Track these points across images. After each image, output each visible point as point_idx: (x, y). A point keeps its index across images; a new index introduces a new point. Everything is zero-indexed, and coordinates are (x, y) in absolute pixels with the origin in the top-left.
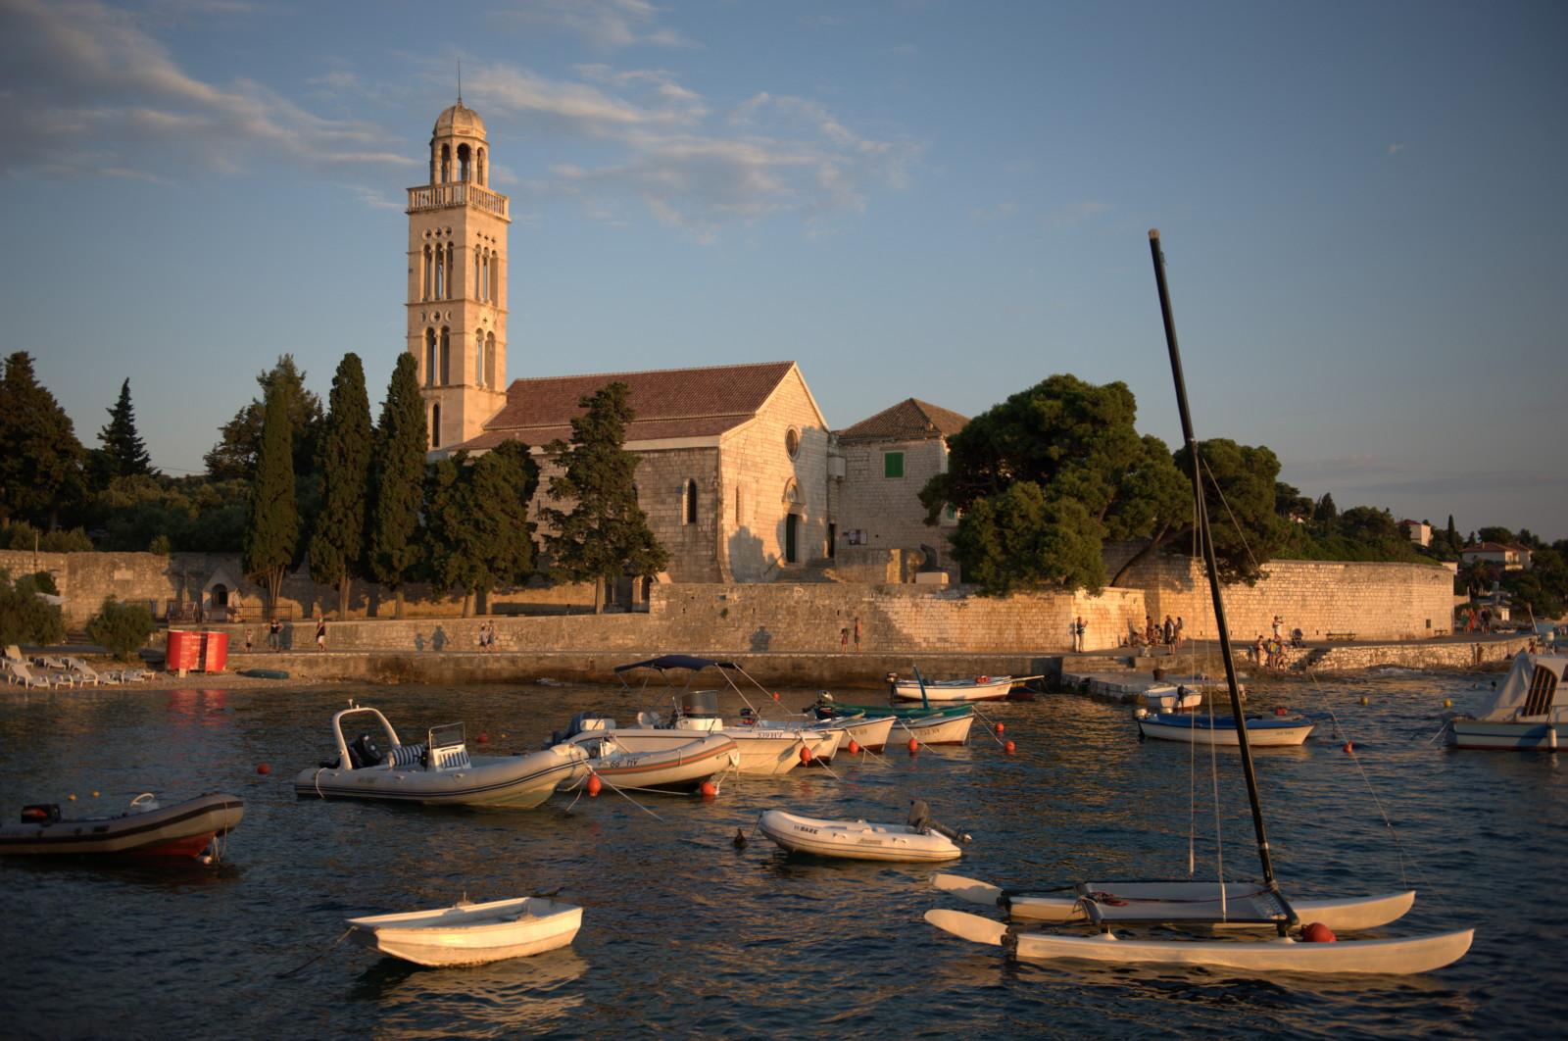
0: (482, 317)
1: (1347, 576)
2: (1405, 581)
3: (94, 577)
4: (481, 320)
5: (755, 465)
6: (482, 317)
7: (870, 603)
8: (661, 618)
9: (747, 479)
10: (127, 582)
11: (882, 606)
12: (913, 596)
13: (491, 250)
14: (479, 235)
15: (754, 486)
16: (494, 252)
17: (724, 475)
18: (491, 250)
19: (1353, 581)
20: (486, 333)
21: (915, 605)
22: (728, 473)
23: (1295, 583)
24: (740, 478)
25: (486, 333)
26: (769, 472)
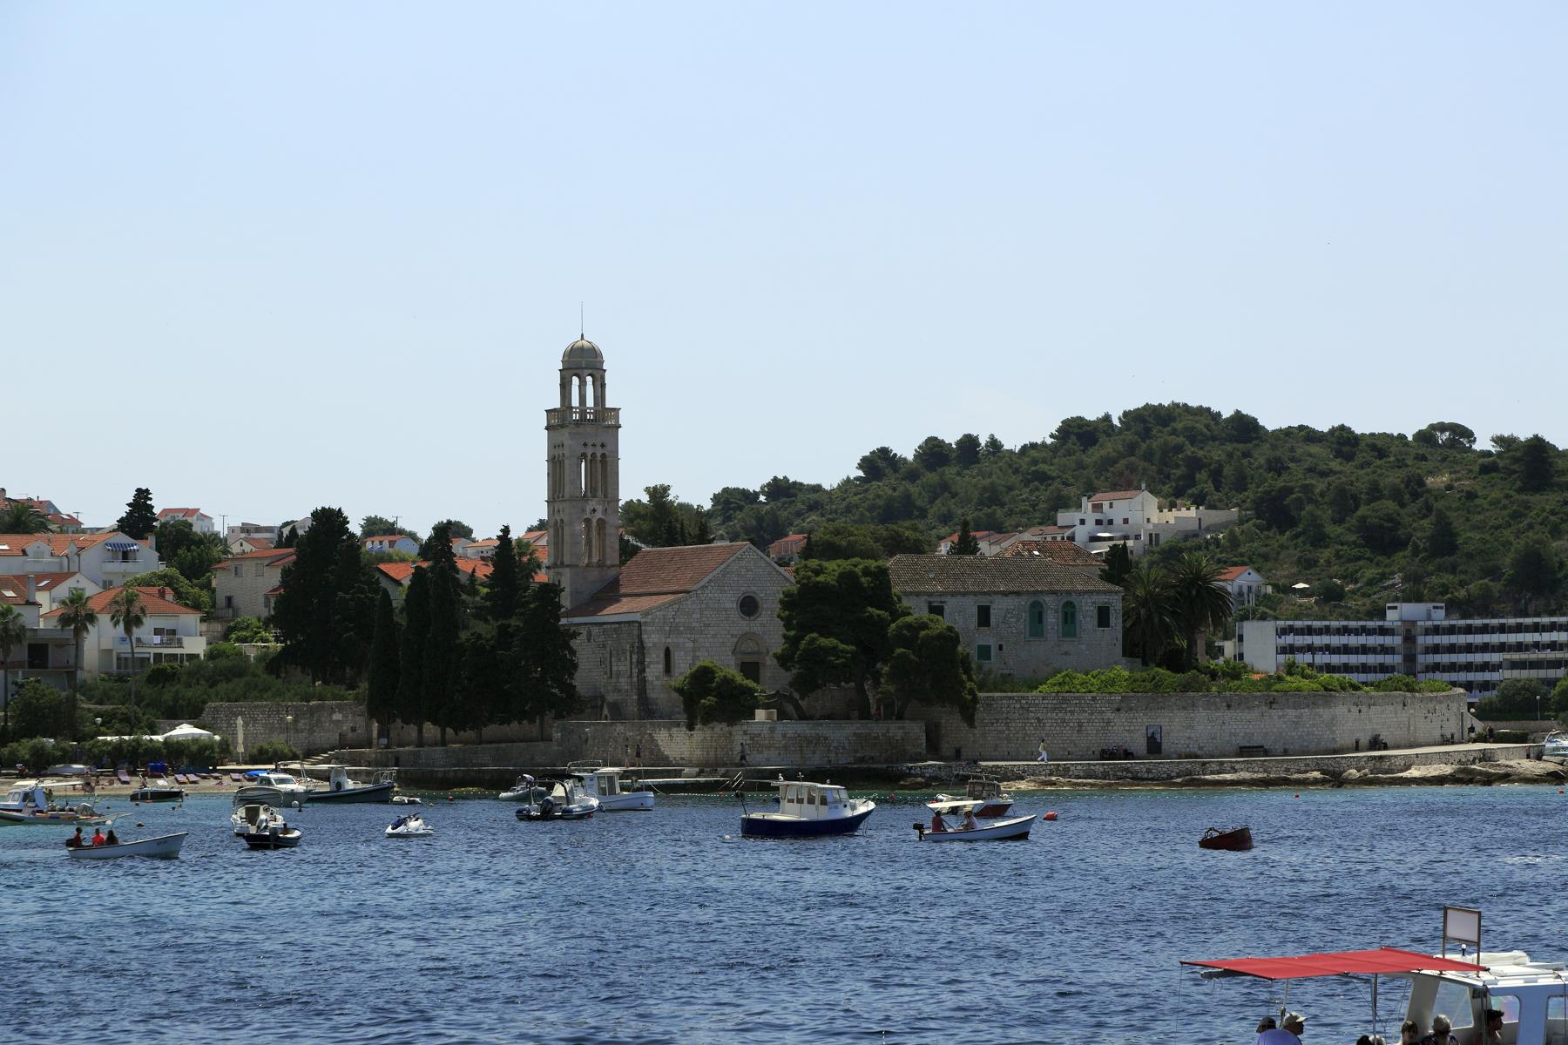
0: (589, 508)
1: (1124, 705)
2: (1185, 708)
3: (323, 719)
4: (588, 511)
5: (691, 630)
6: (589, 508)
7: (650, 734)
8: (558, 745)
9: (681, 640)
10: (339, 721)
11: (656, 736)
12: (669, 729)
13: (599, 455)
14: (585, 445)
15: (691, 645)
16: (603, 455)
17: (647, 641)
18: (599, 455)
19: (1131, 709)
20: (594, 521)
21: (670, 735)
22: (652, 639)
23: (1072, 712)
24: (668, 640)
25: (594, 521)
26: (712, 632)
